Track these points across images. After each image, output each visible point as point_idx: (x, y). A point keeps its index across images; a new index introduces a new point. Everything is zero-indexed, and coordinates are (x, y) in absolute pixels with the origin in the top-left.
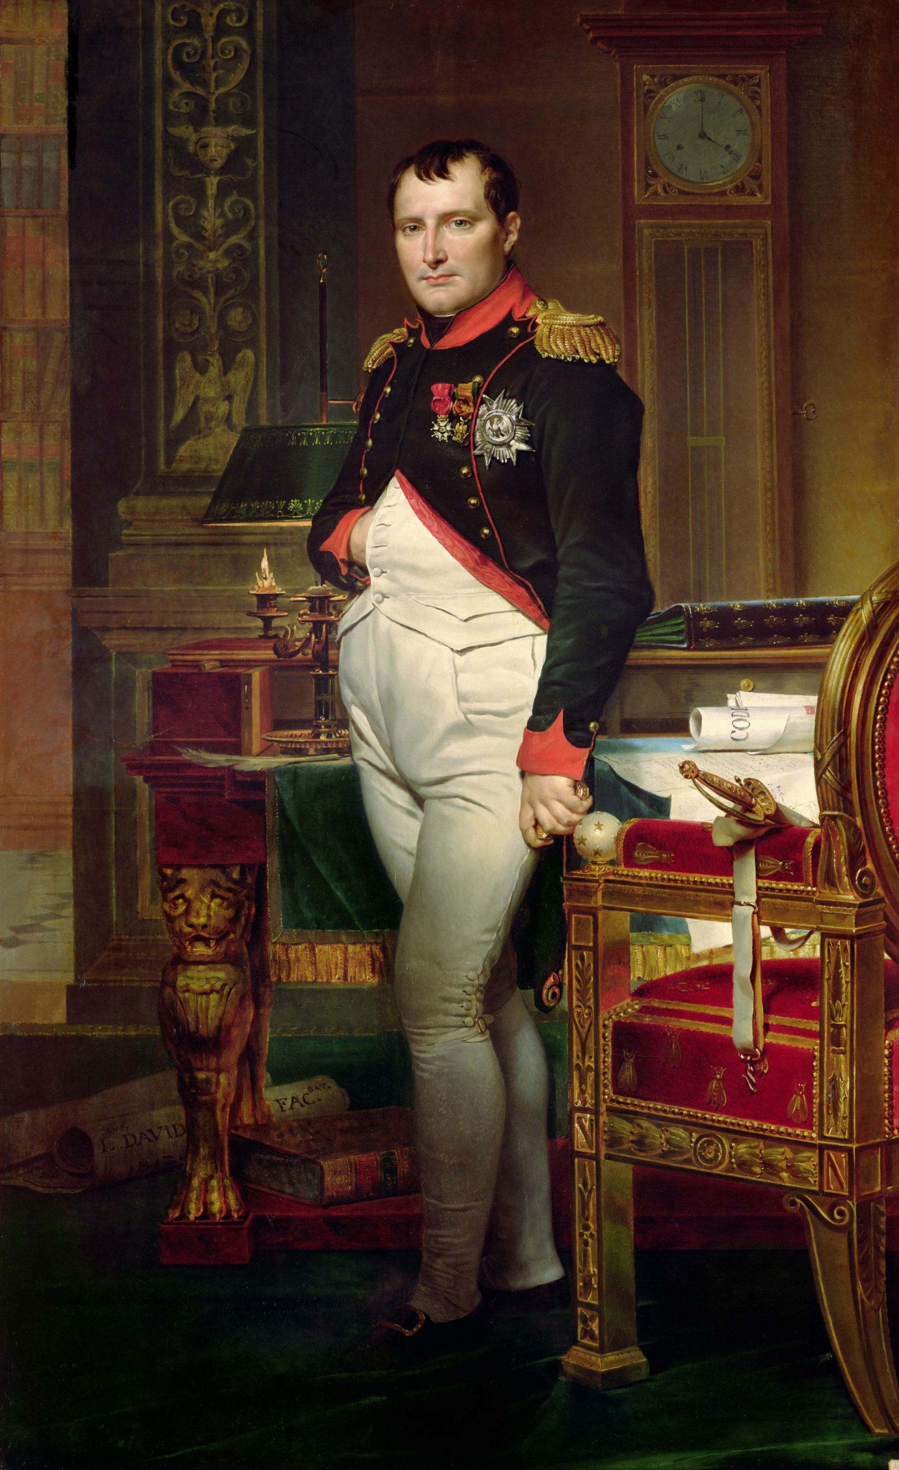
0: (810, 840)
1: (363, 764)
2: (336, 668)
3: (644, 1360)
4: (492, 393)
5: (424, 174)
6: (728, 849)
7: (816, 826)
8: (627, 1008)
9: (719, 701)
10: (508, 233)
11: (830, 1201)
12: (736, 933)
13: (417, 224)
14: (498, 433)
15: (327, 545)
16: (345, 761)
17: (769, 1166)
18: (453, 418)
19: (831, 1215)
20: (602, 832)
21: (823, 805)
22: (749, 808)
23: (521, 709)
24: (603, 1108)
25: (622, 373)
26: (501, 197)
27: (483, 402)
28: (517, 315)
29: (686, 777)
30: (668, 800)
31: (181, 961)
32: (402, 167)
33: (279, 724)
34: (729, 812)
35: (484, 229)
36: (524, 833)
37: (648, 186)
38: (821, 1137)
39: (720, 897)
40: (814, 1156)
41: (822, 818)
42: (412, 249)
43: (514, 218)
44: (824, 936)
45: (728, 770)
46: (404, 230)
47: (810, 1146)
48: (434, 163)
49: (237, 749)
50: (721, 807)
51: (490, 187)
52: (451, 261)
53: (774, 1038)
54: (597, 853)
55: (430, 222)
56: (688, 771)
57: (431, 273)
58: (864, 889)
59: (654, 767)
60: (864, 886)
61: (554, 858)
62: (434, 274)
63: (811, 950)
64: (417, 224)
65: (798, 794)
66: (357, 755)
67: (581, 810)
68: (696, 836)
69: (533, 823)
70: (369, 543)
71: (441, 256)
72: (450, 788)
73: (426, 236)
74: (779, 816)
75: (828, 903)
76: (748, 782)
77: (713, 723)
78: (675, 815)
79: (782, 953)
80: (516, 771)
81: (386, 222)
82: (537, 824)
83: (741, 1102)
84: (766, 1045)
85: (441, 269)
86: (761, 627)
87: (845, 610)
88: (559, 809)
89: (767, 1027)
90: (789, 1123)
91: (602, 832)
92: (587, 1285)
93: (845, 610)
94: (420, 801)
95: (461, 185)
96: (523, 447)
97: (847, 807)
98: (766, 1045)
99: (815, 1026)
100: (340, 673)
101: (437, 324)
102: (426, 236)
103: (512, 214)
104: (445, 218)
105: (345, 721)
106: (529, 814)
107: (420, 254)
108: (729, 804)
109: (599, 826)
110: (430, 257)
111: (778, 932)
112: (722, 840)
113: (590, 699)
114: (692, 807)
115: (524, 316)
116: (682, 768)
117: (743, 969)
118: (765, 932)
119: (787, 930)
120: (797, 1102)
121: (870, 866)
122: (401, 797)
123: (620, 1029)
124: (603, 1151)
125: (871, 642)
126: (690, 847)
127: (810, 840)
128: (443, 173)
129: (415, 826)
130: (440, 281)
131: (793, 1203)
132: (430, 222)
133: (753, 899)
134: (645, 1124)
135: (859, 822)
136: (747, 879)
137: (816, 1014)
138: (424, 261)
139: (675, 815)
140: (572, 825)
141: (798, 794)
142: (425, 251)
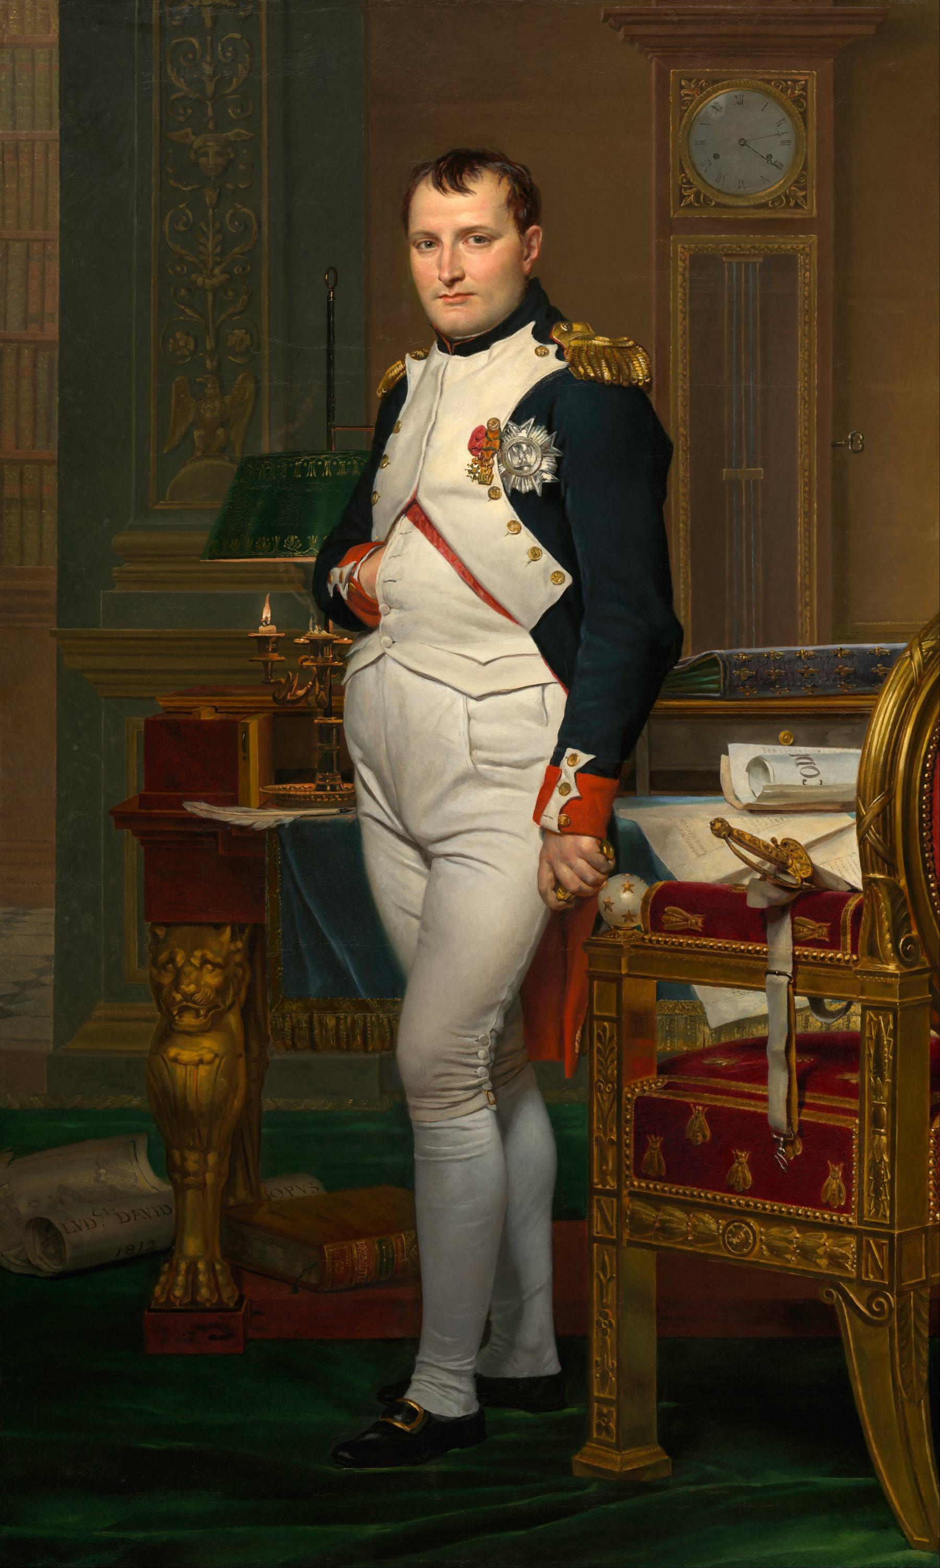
0: (853, 903)
2: (340, 715)
3: (667, 1457)
5: (439, 185)
6: (762, 912)
7: (854, 890)
8: (651, 1085)
10: (530, 248)
13: (432, 240)
16: (349, 817)
21: (864, 869)
22: (783, 868)
23: (540, 760)
24: (625, 1192)
25: (653, 398)
26: (526, 205)
31: (168, 1033)
33: (281, 777)
34: (765, 876)
36: (543, 895)
37: (682, 197)
38: (860, 1220)
39: (752, 963)
40: (852, 1241)
41: (867, 882)
42: (426, 266)
44: (864, 1008)
45: (768, 830)
46: (418, 247)
47: (848, 1231)
48: (454, 171)
49: (233, 801)
51: (512, 201)
53: (809, 1116)
55: (447, 239)
56: (723, 831)
58: (903, 957)
60: (907, 954)
64: (432, 240)
67: (604, 870)
69: (553, 884)
70: (379, 578)
71: (457, 274)
75: (868, 973)
76: (786, 843)
79: (816, 1024)
82: (558, 883)
83: (771, 1183)
84: (801, 1123)
85: (457, 288)
87: (889, 659)
89: (802, 1105)
90: (827, 1207)
91: (625, 896)
92: (604, 1377)
93: (889, 659)
94: (428, 859)
97: (892, 870)
98: (801, 1123)
104: (464, 234)
105: (349, 774)
106: (548, 876)
107: (436, 273)
109: (629, 889)
110: (446, 275)
111: (817, 1005)
112: (755, 901)
116: (712, 825)
117: (777, 1045)
118: (801, 1001)
119: (826, 1001)
121: (915, 933)
122: (409, 855)
123: (642, 1104)
124: (626, 1236)
127: (853, 903)
128: (461, 189)
130: (457, 299)
131: (829, 1294)
133: (789, 970)
134: (670, 1209)
135: (903, 883)
136: (782, 944)
137: (853, 1091)
142: (440, 267)
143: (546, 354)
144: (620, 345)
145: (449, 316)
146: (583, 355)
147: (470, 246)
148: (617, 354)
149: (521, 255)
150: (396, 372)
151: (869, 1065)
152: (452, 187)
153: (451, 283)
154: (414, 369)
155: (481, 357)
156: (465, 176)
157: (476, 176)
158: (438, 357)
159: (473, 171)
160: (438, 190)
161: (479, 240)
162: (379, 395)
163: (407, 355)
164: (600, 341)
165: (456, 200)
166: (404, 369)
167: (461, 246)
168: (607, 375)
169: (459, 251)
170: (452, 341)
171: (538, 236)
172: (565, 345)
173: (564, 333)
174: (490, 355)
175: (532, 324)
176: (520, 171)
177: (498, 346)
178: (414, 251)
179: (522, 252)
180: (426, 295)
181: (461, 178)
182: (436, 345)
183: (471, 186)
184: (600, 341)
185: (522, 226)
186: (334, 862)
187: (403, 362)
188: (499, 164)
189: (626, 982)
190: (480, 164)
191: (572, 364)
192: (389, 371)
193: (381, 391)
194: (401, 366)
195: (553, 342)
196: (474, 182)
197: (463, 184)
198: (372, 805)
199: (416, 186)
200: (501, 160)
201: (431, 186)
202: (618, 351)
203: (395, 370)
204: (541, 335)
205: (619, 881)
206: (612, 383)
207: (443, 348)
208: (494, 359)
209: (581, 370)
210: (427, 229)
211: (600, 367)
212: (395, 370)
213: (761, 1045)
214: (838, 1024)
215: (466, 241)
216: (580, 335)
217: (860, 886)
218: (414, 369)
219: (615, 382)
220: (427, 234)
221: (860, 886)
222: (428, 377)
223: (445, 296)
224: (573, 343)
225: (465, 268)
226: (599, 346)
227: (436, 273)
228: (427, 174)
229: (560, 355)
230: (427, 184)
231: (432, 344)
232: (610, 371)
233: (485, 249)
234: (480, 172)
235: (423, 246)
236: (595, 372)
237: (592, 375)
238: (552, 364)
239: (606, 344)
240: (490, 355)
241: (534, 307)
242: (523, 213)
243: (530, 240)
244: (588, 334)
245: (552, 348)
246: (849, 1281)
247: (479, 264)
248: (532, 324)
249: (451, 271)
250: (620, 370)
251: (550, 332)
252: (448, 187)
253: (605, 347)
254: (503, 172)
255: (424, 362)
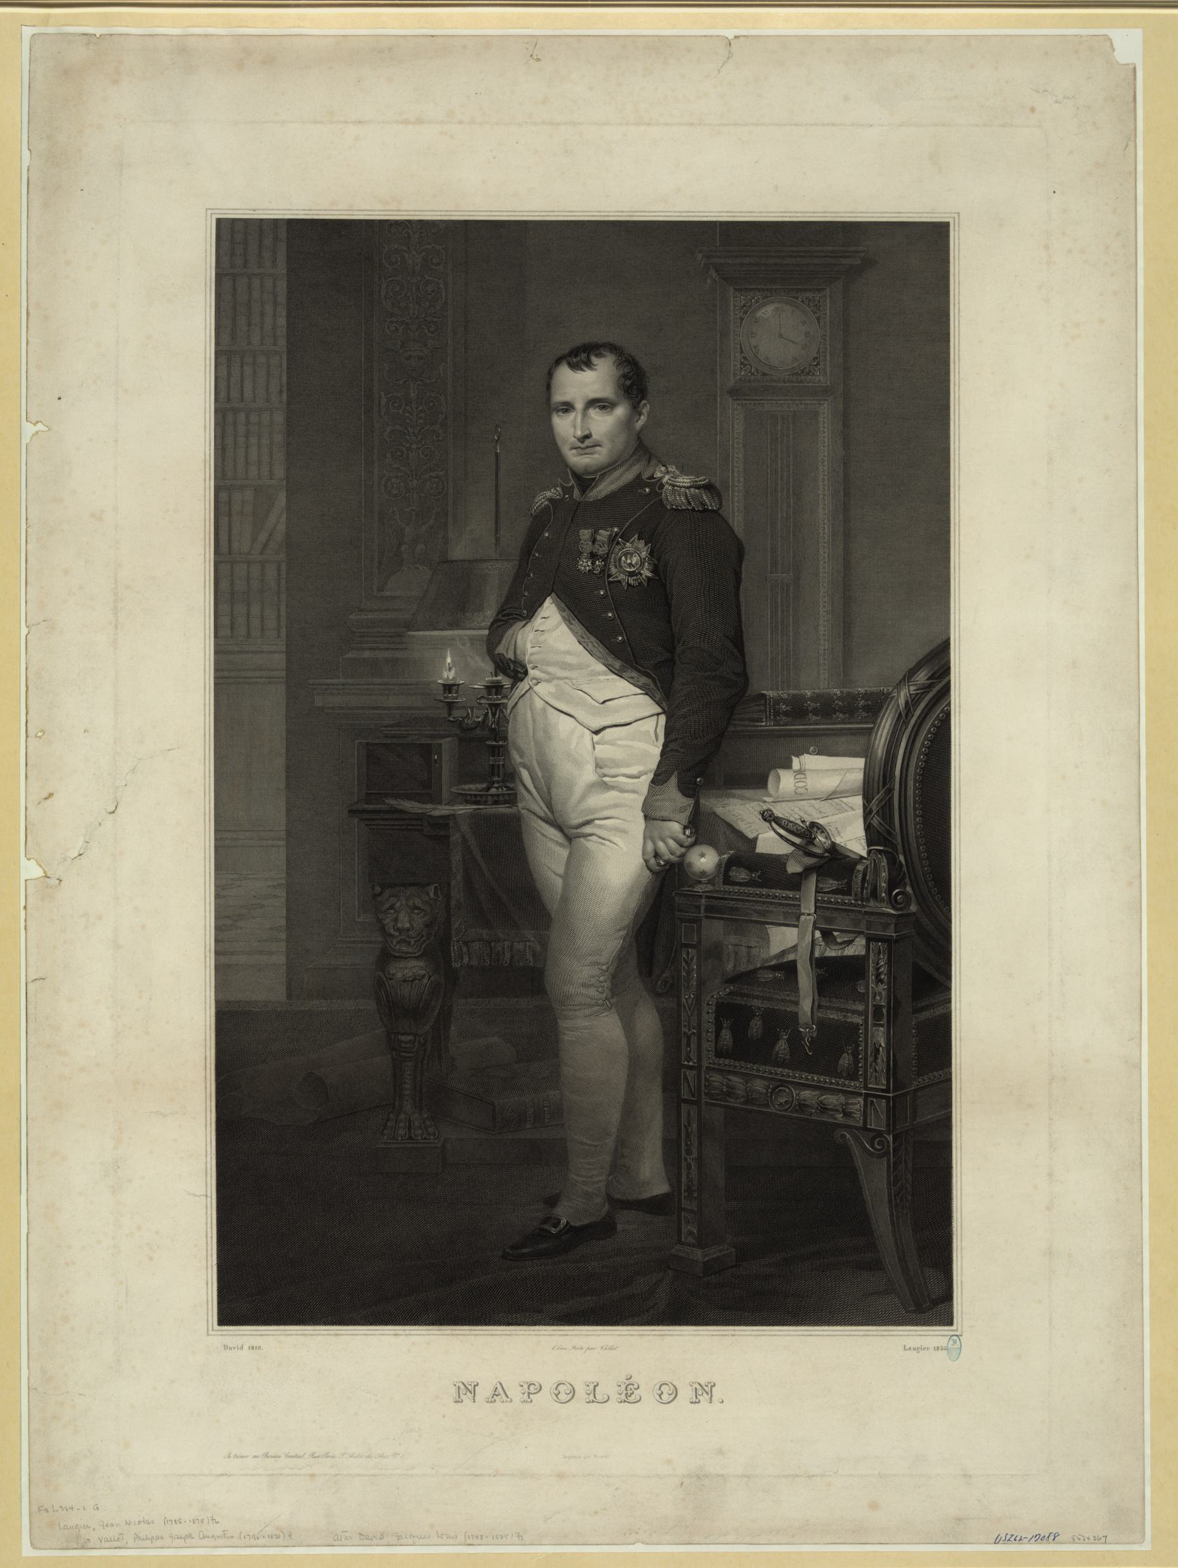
1: (523, 811)
4: (626, 537)
7: (862, 858)
9: (788, 766)
11: (872, 1135)
12: (801, 936)
13: (567, 407)
14: (630, 565)
15: (500, 649)
17: (823, 1109)
18: (593, 556)
19: (873, 1147)
20: (705, 860)
21: (870, 842)
26: (634, 386)
27: (618, 543)
28: (645, 476)
29: (765, 820)
30: (756, 839)
32: (558, 362)
35: (620, 411)
36: (646, 861)
40: (861, 1100)
41: (869, 852)
42: (565, 427)
49: (436, 800)
50: (793, 844)
54: (703, 873)
56: (769, 817)
57: (579, 444)
59: (742, 812)
61: (667, 881)
62: (583, 446)
63: (857, 948)
64: (567, 407)
65: (852, 836)
66: (520, 805)
68: (777, 862)
71: (586, 432)
72: (587, 830)
73: (575, 419)
74: (834, 849)
77: (786, 781)
78: (761, 848)
80: (642, 814)
81: (547, 406)
82: (657, 855)
85: (587, 442)
86: (826, 708)
88: (671, 843)
94: (569, 839)
96: (649, 575)
99: (861, 1008)
100: (510, 747)
101: (585, 480)
102: (575, 419)
104: (592, 403)
106: (650, 847)
108: (797, 840)
109: (703, 855)
110: (579, 433)
112: (793, 868)
113: (709, 753)
114: (770, 842)
115: (652, 477)
116: (762, 814)
120: (845, 1060)
125: (906, 723)
126: (768, 871)
127: (860, 867)
129: (564, 853)
130: (588, 451)
131: (843, 1136)
132: (579, 406)
137: (863, 998)
139: (761, 848)
140: (683, 856)
141: (852, 836)
142: (575, 427)
151: (872, 978)
186: (504, 840)
189: (705, 922)
198: (530, 802)
205: (698, 849)
213: (793, 964)
214: (850, 951)
217: (864, 854)
221: (864, 854)
227: (572, 431)
246: (855, 1127)
247: (603, 424)
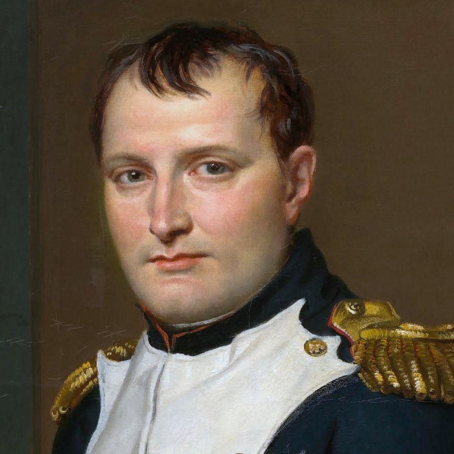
10: (297, 182)
13: (140, 169)
26: (290, 113)
43: (306, 156)
46: (117, 179)
48: (174, 59)
51: (267, 107)
52: (196, 232)
55: (163, 167)
57: (161, 250)
71: (179, 223)
85: (180, 246)
95: (215, 108)
103: (302, 149)
104: (189, 158)
107: (146, 222)
110: (162, 225)
128: (187, 88)
130: (179, 264)
138: (152, 232)
142: (152, 212)
143: (322, 351)
144: (440, 337)
145: (167, 291)
146: (382, 353)
147: (201, 179)
148: (436, 352)
149: (282, 194)
150: (81, 379)
152: (172, 84)
153: (171, 237)
154: (111, 375)
155: (219, 356)
156: (192, 66)
157: (210, 66)
158: (149, 357)
159: (205, 58)
160: (150, 88)
161: (214, 168)
162: (55, 417)
163: (100, 354)
164: (409, 331)
165: (177, 105)
166: (95, 375)
167: (186, 178)
168: (419, 385)
169: (182, 186)
170: (171, 331)
171: (310, 161)
172: (353, 337)
173: (351, 317)
174: (233, 353)
175: (300, 304)
176: (280, 57)
177: (245, 339)
178: (111, 186)
179: (284, 187)
180: (130, 257)
181: (186, 70)
182: (145, 337)
183: (202, 82)
184: (409, 331)
185: (284, 146)
187: (94, 365)
188: (246, 47)
190: (216, 47)
191: (364, 367)
192: (70, 378)
193: (57, 411)
194: (90, 371)
195: (333, 332)
196: (207, 75)
197: (189, 79)
199: (114, 82)
200: (250, 41)
201: (137, 82)
202: (437, 347)
203: (80, 378)
204: (315, 321)
206: (428, 399)
207: (157, 342)
208: (238, 360)
209: (378, 376)
210: (132, 151)
211: (409, 371)
212: (80, 378)
215: (194, 171)
216: (377, 321)
218: (111, 375)
219: (433, 397)
220: (132, 159)
222: (133, 390)
223: (161, 259)
224: (366, 335)
225: (192, 214)
226: (407, 339)
227: (146, 222)
228: (130, 63)
229: (344, 353)
230: (131, 79)
231: (139, 336)
232: (425, 378)
233: (224, 184)
234: (216, 61)
235: (125, 178)
236: (400, 380)
237: (396, 384)
238: (332, 368)
239: (419, 335)
240: (233, 353)
241: (306, 275)
242: (285, 126)
243: (297, 168)
244: (389, 319)
245: (332, 343)
248: (300, 304)
249: (170, 219)
250: (440, 377)
251: (329, 315)
252: (164, 83)
253: (416, 341)
254: (253, 60)
255: (126, 364)
